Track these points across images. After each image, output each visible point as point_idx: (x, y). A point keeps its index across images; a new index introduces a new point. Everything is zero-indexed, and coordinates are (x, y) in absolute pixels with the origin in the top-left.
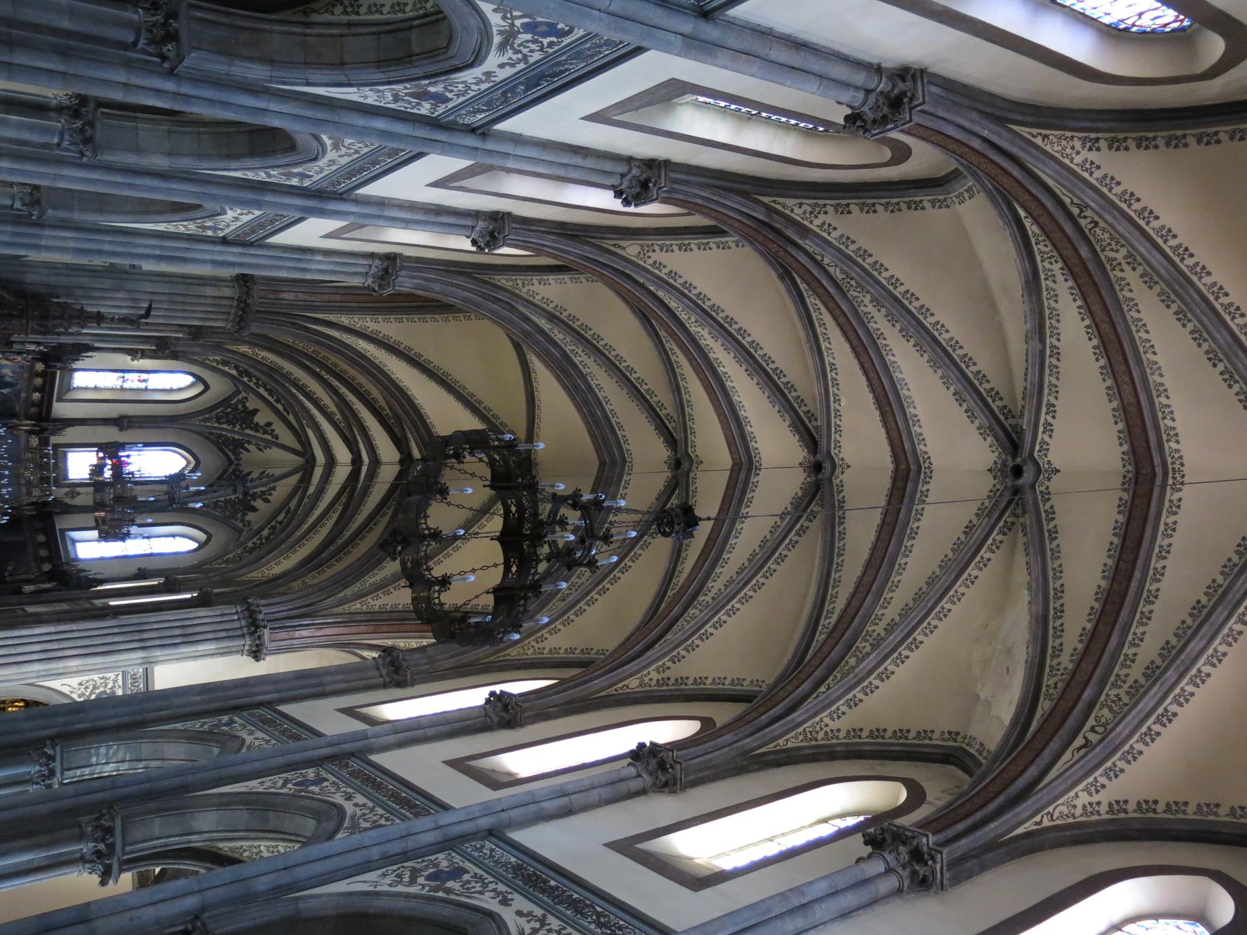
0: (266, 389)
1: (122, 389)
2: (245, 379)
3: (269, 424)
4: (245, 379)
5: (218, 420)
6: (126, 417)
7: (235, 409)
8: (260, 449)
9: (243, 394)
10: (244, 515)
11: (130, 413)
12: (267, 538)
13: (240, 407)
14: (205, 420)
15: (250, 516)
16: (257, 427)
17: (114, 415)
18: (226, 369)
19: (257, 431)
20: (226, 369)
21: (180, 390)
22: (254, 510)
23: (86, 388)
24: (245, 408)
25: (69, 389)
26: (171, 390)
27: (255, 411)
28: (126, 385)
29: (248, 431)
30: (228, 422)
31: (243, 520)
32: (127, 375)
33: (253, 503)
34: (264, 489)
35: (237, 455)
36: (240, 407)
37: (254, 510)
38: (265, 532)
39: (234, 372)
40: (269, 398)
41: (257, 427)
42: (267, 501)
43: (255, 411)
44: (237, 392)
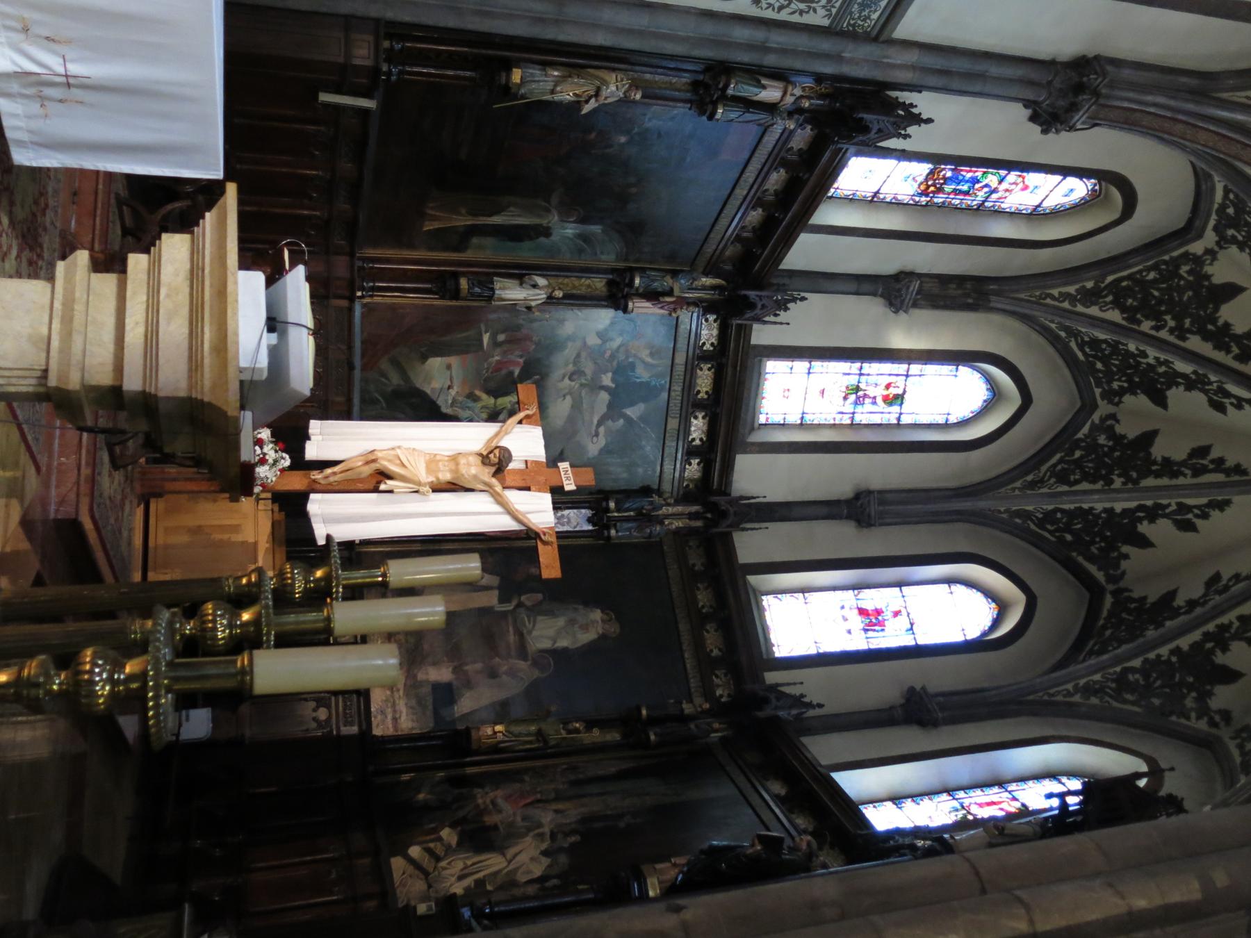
0: (1206, 336)
1: (853, 426)
2: (1146, 326)
3: (1203, 451)
4: (1146, 326)
5: (1063, 478)
6: (869, 492)
7: (1092, 447)
9: (1104, 408)
10: (1204, 696)
11: (876, 484)
13: (1102, 440)
14: (1033, 485)
15: (1223, 696)
16: (1169, 468)
17: (842, 489)
18: (1094, 311)
19: (1175, 475)
20: (1094, 311)
22: (1230, 676)
23: (783, 426)
24: (1118, 439)
25: (753, 427)
26: (946, 426)
27: (1148, 438)
28: (861, 418)
29: (1150, 482)
30: (1086, 477)
31: (1203, 711)
32: (869, 367)
33: (1220, 658)
35: (1110, 561)
36: (1102, 440)
39: (1115, 316)
40: (1219, 356)
43: (1148, 438)
44: (1088, 407)
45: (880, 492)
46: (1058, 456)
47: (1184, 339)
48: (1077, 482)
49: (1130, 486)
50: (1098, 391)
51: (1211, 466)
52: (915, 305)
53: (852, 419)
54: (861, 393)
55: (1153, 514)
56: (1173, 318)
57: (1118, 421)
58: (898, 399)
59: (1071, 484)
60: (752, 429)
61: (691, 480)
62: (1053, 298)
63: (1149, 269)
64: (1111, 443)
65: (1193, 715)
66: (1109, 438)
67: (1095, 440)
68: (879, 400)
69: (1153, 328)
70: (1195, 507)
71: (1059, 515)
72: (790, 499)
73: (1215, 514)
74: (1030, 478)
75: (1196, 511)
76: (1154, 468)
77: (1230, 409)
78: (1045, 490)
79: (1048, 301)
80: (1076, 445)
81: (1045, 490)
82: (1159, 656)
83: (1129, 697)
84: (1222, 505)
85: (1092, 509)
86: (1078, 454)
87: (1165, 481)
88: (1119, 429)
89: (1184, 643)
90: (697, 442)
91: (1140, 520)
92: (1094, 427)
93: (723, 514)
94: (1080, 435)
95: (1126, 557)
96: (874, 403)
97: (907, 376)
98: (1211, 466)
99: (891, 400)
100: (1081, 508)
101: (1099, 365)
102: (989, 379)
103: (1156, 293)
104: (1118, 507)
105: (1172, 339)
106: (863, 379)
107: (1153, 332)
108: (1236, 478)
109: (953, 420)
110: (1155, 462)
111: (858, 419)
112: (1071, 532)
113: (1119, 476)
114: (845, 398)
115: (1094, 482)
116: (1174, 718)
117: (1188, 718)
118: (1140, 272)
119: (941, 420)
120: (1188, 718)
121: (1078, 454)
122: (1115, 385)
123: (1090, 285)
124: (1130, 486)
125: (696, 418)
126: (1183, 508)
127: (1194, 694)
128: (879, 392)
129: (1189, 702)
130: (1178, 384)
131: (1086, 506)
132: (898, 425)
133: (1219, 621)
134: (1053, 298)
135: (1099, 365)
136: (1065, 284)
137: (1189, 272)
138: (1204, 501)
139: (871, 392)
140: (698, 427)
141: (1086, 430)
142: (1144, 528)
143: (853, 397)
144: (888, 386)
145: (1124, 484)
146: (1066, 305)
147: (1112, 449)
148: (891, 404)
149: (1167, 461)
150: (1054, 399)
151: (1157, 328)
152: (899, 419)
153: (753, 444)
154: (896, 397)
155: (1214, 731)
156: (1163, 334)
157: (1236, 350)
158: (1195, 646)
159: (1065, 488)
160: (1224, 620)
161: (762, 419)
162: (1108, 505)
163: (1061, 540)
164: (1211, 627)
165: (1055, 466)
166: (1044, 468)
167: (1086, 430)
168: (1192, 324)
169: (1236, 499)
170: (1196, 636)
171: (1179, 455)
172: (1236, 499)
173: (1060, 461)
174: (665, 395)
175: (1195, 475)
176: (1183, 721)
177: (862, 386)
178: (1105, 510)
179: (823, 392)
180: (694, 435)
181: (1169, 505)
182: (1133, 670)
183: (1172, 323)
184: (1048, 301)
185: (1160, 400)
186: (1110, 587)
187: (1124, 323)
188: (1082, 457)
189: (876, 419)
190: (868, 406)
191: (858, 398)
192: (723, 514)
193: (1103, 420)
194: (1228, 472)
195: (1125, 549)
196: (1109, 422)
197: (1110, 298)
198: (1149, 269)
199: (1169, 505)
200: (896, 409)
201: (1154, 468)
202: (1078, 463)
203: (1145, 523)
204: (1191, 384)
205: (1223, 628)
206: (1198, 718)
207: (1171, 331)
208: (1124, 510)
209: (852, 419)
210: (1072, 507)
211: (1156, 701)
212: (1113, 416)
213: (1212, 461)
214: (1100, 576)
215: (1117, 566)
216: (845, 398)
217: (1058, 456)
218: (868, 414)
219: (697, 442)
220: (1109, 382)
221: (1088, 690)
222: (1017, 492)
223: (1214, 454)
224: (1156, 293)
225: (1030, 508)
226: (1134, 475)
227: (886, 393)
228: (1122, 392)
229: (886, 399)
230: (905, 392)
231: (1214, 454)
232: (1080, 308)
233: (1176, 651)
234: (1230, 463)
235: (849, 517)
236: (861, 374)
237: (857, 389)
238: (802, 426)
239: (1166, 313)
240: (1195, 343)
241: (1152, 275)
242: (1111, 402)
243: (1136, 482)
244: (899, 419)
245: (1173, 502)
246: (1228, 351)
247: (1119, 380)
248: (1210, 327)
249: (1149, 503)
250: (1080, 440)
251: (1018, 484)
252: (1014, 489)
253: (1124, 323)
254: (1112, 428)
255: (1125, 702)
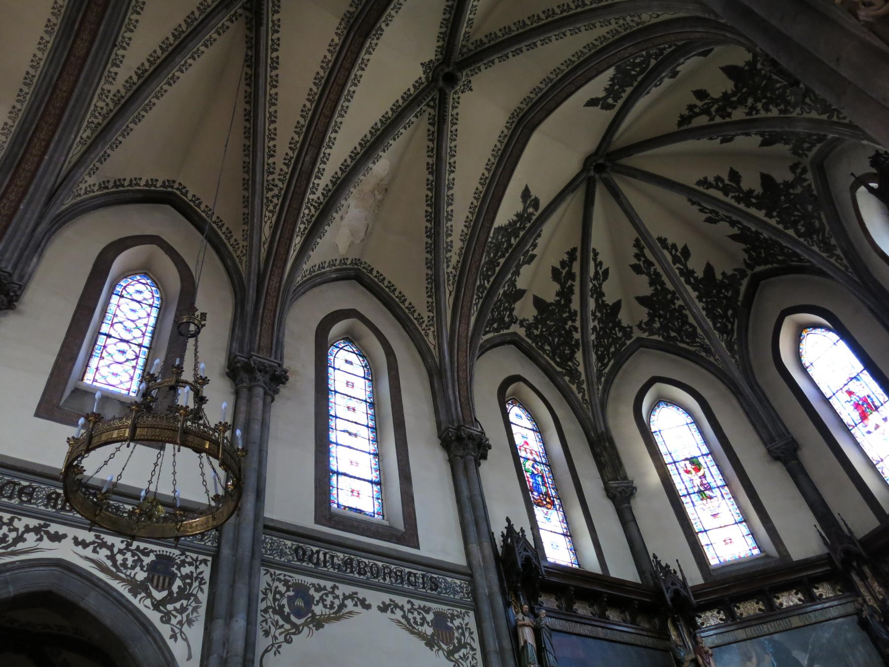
3: (636, 269)
4: (577, 336)
5: (693, 335)
6: (770, 452)
7: (665, 328)
8: (686, 252)
9: (637, 334)
10: (788, 185)
11: (761, 450)
12: (742, 102)
13: (657, 325)
14: (707, 350)
15: (782, 175)
16: (656, 279)
17: (778, 471)
18: (581, 369)
19: (658, 275)
20: (581, 369)
21: (688, 411)
22: (767, 180)
23: (753, 534)
26: (696, 422)
27: (642, 301)
29: (669, 286)
30: (685, 320)
31: (800, 180)
33: (759, 190)
34: (719, 194)
35: (732, 282)
36: (657, 325)
37: (767, 180)
38: (738, 114)
39: (579, 356)
41: (656, 279)
42: (735, 176)
43: (642, 301)
44: (642, 343)
45: (765, 444)
46: (681, 345)
47: (576, 312)
48: (691, 326)
49: (677, 295)
50: (628, 342)
51: (643, 259)
52: (625, 478)
53: (723, 486)
54: (702, 489)
55: (688, 274)
56: (566, 324)
57: (641, 322)
58: (694, 461)
59: (695, 328)
60: (767, 556)
61: (834, 590)
62: (584, 396)
63: (544, 351)
64: (657, 319)
65: (805, 184)
66: (654, 322)
67: (659, 329)
68: (700, 473)
69: (577, 332)
70: (671, 254)
71: (719, 325)
72: (805, 506)
73: (670, 242)
74: (703, 354)
75: (674, 252)
76: (659, 288)
77: (604, 267)
78: (707, 341)
79: (587, 397)
80: (668, 338)
81: (707, 341)
82: (778, 223)
83: (817, 224)
84: (663, 241)
85: (704, 309)
86: (673, 334)
87: (664, 278)
88: (646, 319)
89: (761, 214)
90: (800, 596)
91: (696, 279)
92: (652, 333)
93: (847, 552)
94: (661, 339)
95: (724, 274)
96: (704, 476)
97: (675, 462)
98: (643, 259)
99: (697, 467)
100: (707, 315)
101: (612, 349)
102: (652, 409)
103: (556, 340)
104: (694, 294)
105: (578, 318)
106: (691, 491)
107: (579, 330)
108: (642, 243)
109: (689, 420)
110: (656, 289)
111: (721, 483)
112: (726, 312)
113: (674, 304)
114: (711, 498)
115: (686, 316)
116: (815, 192)
117: (810, 185)
118: (548, 355)
119: (693, 427)
120: (810, 185)
121: (673, 334)
122: (620, 335)
123: (567, 379)
124: (677, 295)
125: (781, 604)
126: (676, 260)
127: (791, 191)
128: (696, 478)
129: (799, 190)
130: (603, 302)
131: (704, 313)
132: (711, 453)
133: (736, 204)
134: (584, 396)
135: (612, 349)
136: (573, 393)
137: (537, 329)
138: (665, 252)
139: (697, 482)
140: (788, 600)
141: (656, 337)
142: (700, 274)
143: (708, 493)
144: (688, 472)
145: (678, 299)
146: (585, 386)
147: (660, 316)
148: (699, 464)
149: (651, 284)
150: (645, 365)
151: (576, 329)
152: (707, 455)
153: (779, 552)
154: (692, 463)
155: (809, 168)
156: (578, 324)
157: (570, 283)
158: (759, 207)
159: (699, 330)
160: (733, 202)
161: (756, 552)
162: (697, 301)
163: (733, 316)
164: (742, 206)
165: (688, 344)
166: (693, 349)
167: (656, 337)
168: (565, 312)
169: (655, 236)
170: (753, 211)
171: (645, 279)
172: (655, 236)
173: (682, 341)
174: (776, 637)
175: (653, 264)
176: (813, 187)
177: (696, 489)
178: (700, 301)
179: (714, 515)
180: (796, 601)
181: (678, 268)
182: (797, 232)
183: (570, 323)
184: (587, 397)
185: (617, 306)
186: (749, 272)
187: (581, 349)
188: (674, 331)
189: (715, 470)
190: (709, 479)
191: (706, 489)
192: (847, 552)
193: (644, 331)
194: (641, 249)
195: (719, 277)
196: (644, 326)
197: (570, 363)
198: (544, 351)
199: (678, 268)
200: (701, 460)
201: (659, 288)
202: (679, 331)
203: (696, 275)
204: (599, 294)
205: (738, 199)
206: (806, 180)
207: (574, 321)
208: (695, 290)
209: (723, 486)
210: (708, 320)
211: (810, 208)
212: (639, 326)
213: (639, 260)
214: (745, 282)
215: (733, 275)
216: (711, 498)
217: (681, 345)
218: (715, 478)
219: (800, 596)
220: (620, 339)
221: (828, 248)
222: (717, 357)
223: (634, 261)
224: (556, 340)
225: (723, 344)
226: (669, 296)
227: (693, 472)
228: (622, 329)
229: (697, 469)
230: (686, 459)
231: (634, 261)
232: (583, 377)
233: (769, 215)
234: (636, 251)
235: (796, 458)
236: (689, 494)
237: (700, 492)
238: (746, 520)
239: (564, 329)
240: (575, 305)
241: (547, 347)
242: (631, 332)
243: (673, 293)
244: (707, 455)
245: (675, 267)
246: (572, 285)
247: (616, 334)
248: (563, 302)
249: (683, 279)
250: (663, 337)
251: (712, 359)
252: (716, 360)
253: (581, 349)
254: (646, 324)
255: (821, 223)
